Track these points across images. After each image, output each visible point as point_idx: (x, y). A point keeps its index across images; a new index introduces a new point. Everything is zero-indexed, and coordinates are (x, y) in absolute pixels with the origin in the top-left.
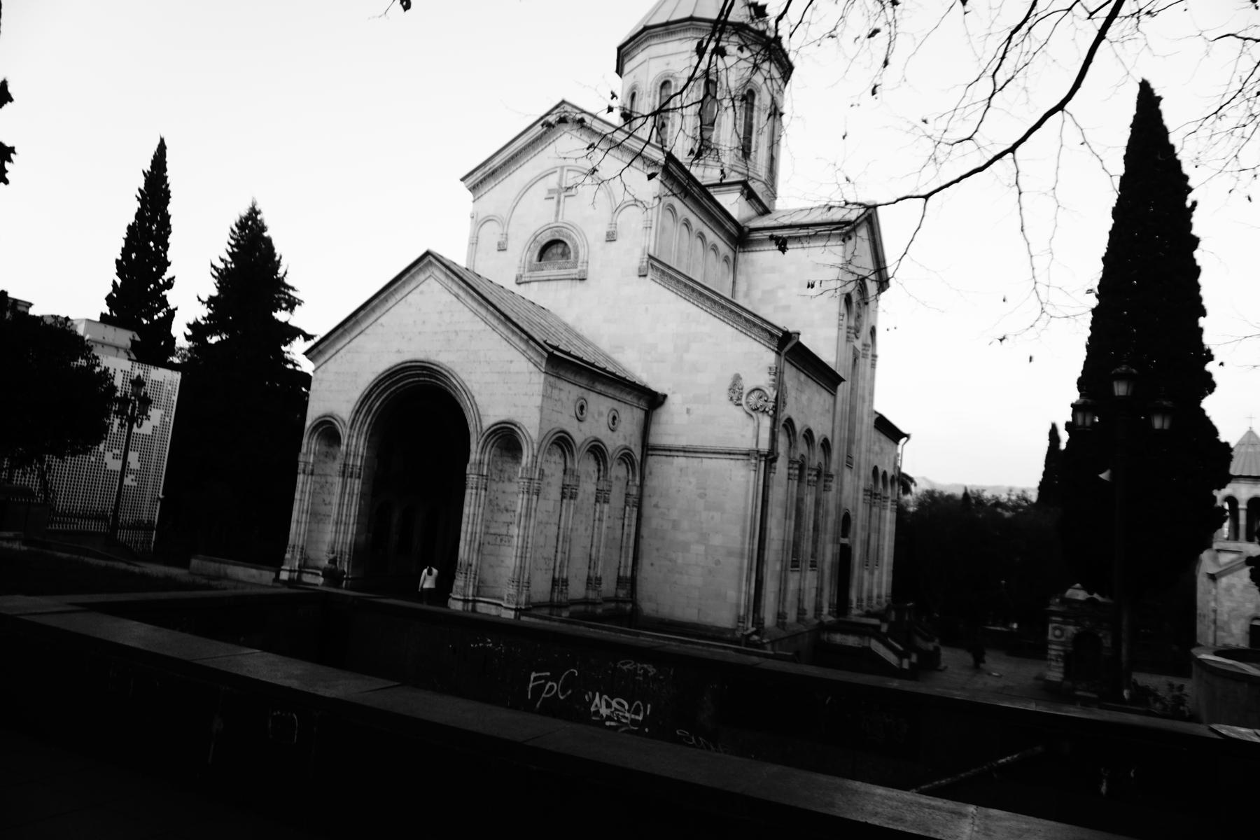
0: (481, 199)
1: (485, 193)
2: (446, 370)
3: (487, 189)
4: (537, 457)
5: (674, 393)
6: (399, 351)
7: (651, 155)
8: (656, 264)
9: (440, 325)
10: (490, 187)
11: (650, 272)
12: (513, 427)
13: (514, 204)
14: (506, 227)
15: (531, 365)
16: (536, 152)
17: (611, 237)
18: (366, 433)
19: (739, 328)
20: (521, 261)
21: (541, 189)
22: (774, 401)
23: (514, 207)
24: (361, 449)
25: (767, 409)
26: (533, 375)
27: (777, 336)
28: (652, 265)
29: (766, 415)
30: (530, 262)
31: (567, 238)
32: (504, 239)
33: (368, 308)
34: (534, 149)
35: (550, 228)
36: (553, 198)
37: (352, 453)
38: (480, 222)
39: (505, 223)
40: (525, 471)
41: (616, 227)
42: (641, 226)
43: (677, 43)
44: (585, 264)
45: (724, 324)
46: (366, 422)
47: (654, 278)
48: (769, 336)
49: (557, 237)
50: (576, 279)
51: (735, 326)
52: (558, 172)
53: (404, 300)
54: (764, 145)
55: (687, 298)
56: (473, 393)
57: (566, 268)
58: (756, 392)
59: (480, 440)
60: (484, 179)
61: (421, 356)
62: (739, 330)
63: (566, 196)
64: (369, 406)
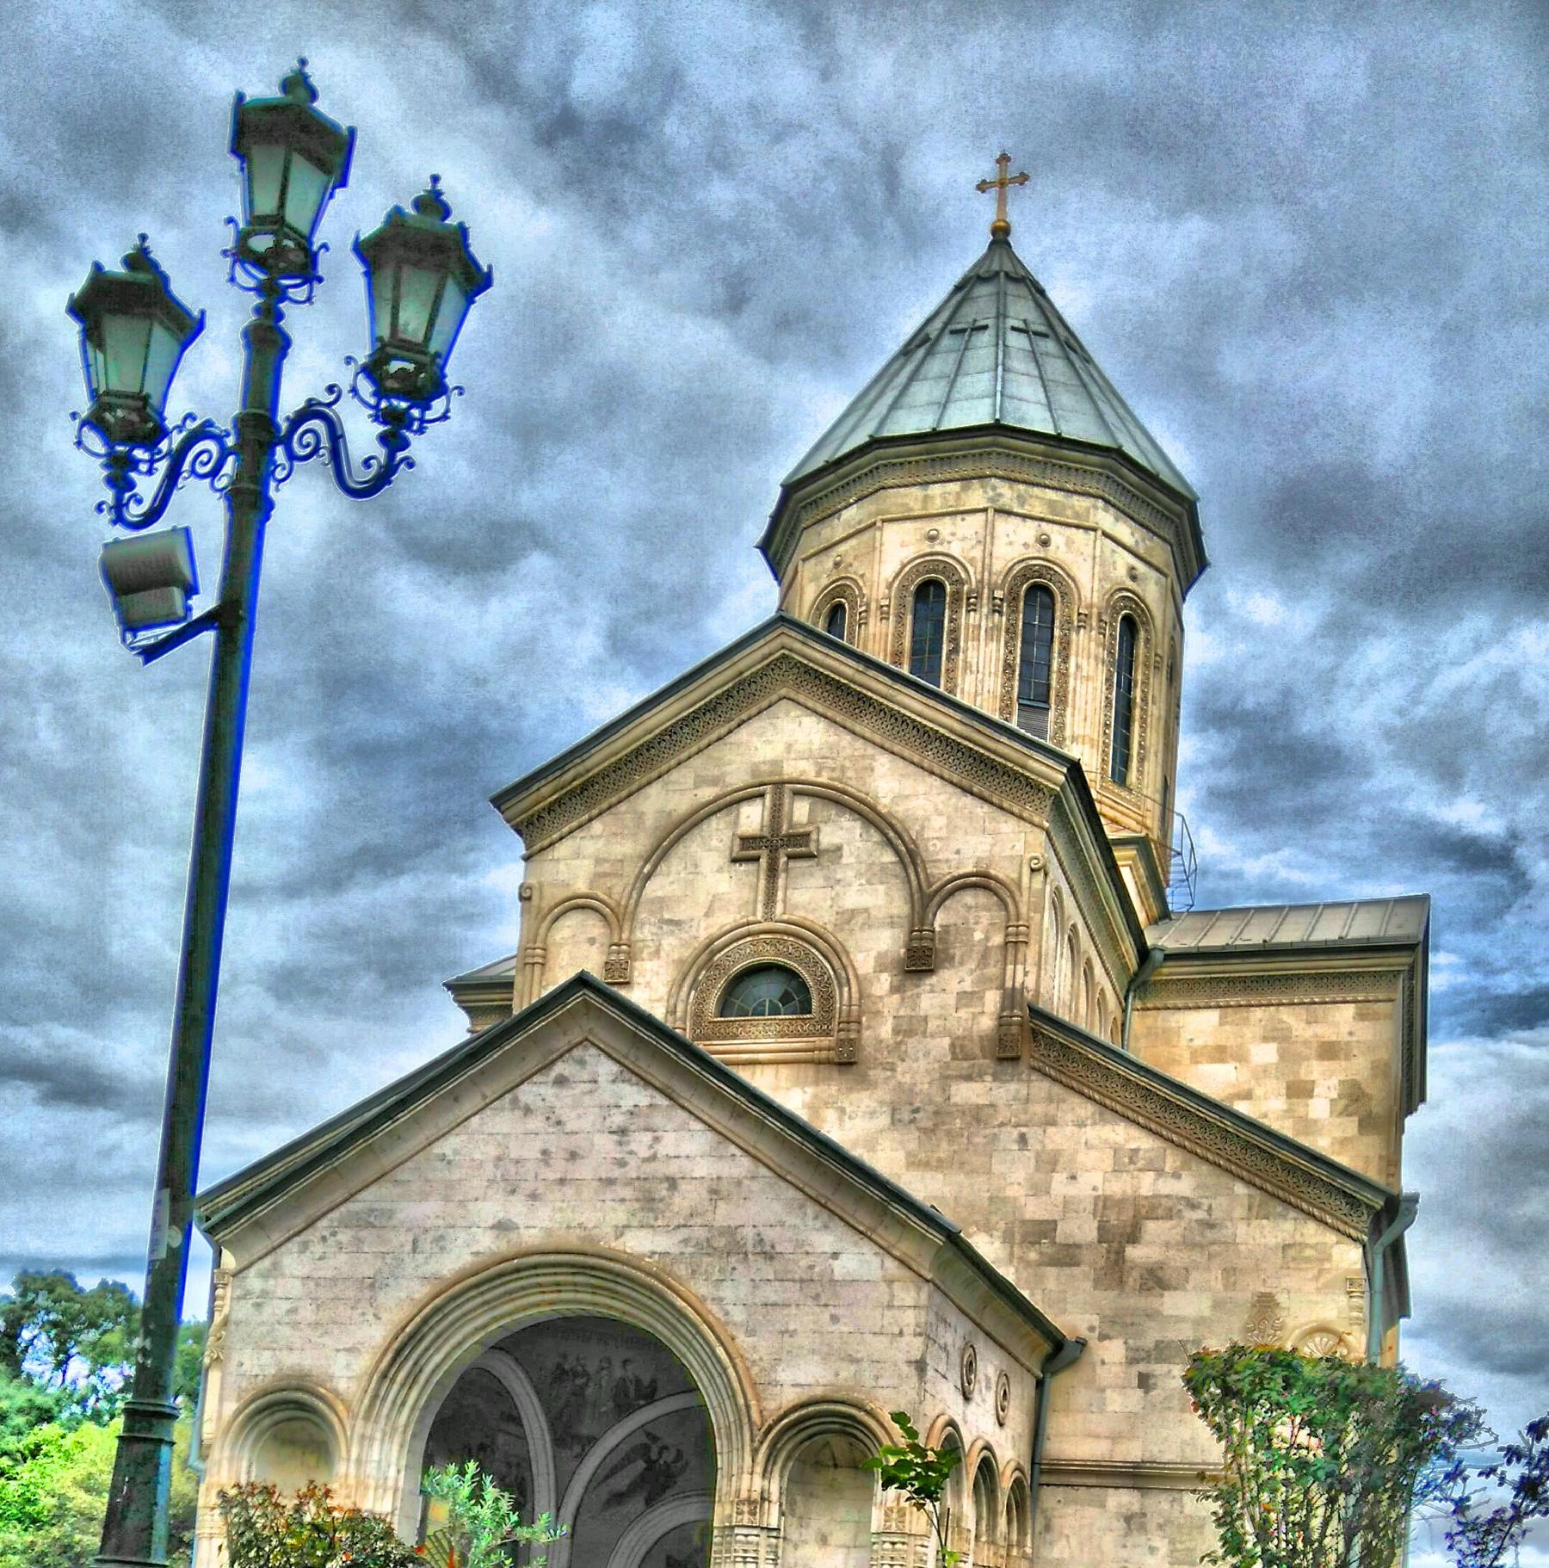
0: (549, 855)
1: (561, 839)
2: (648, 1274)
3: (566, 830)
6: (502, 1227)
8: (1048, 1030)
9: (622, 1163)
10: (575, 824)
11: (1025, 1050)
12: (853, 1411)
14: (626, 926)
15: (891, 1264)
18: (405, 1432)
19: (1269, 1187)
20: (674, 1012)
23: (649, 877)
24: (392, 1472)
26: (896, 1285)
27: (1368, 1206)
28: (1035, 1033)
30: (698, 1016)
32: (622, 957)
36: (756, 859)
37: (372, 1483)
38: (551, 910)
40: (894, 1516)
41: (932, 940)
42: (997, 939)
43: (954, 487)
44: (854, 1026)
45: (1225, 1179)
46: (403, 1404)
47: (1036, 1064)
48: (1346, 1209)
49: (769, 957)
50: (828, 1062)
51: (1258, 1181)
52: (768, 797)
55: (1130, 1114)
56: (731, 1330)
57: (800, 1036)
59: (762, 1443)
60: (559, 802)
61: (573, 1240)
62: (1266, 1191)
63: (791, 857)
64: (415, 1364)
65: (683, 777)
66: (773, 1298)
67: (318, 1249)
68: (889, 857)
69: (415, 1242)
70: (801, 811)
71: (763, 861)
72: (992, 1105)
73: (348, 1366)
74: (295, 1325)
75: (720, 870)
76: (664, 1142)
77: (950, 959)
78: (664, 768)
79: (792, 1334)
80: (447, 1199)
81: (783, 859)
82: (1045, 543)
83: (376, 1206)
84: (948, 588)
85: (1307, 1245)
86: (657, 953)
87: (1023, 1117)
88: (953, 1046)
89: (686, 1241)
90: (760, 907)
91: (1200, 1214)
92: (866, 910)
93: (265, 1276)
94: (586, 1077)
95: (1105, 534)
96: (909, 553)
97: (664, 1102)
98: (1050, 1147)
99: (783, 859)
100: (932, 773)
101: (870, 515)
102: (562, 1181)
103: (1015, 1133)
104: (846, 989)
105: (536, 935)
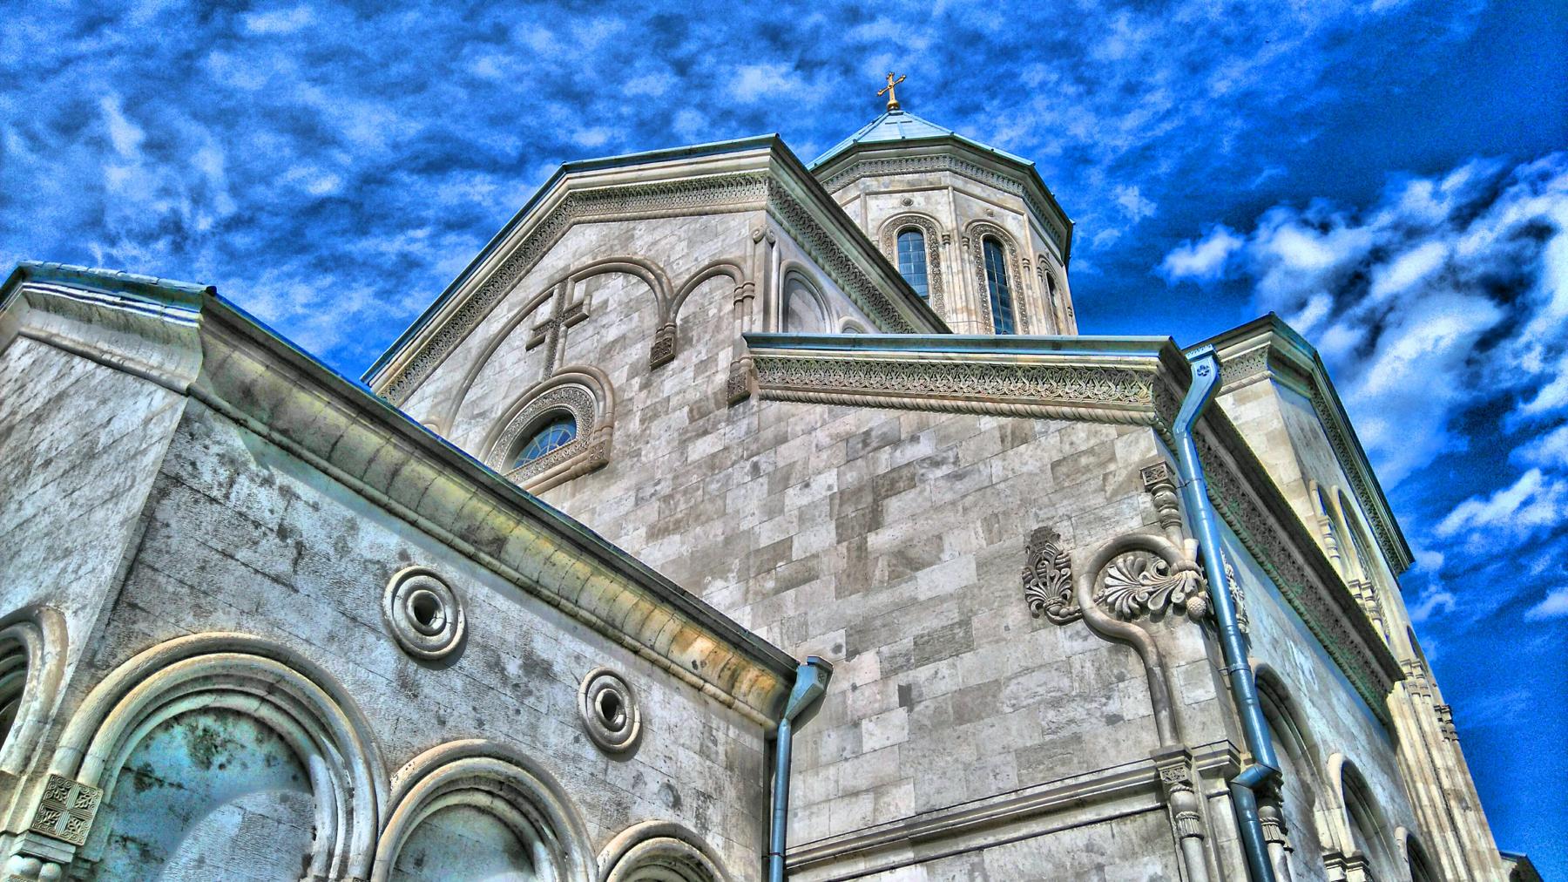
4: (60, 722)
5: (852, 654)
7: (738, 168)
17: (662, 356)
21: (523, 334)
22: (1196, 565)
25: (1177, 597)
29: (1179, 619)
31: (568, 399)
34: (512, 276)
35: (533, 397)
36: (542, 341)
42: (729, 306)
49: (546, 405)
50: (584, 472)
54: (1039, 321)
58: (1120, 561)
60: (413, 365)
63: (569, 326)
72: (726, 449)
77: (689, 341)
81: (563, 328)
82: (908, 203)
85: (1084, 453)
87: (754, 447)
88: (691, 411)
91: (945, 470)
95: (954, 189)
98: (781, 464)
99: (563, 328)
103: (748, 465)
104: (601, 404)
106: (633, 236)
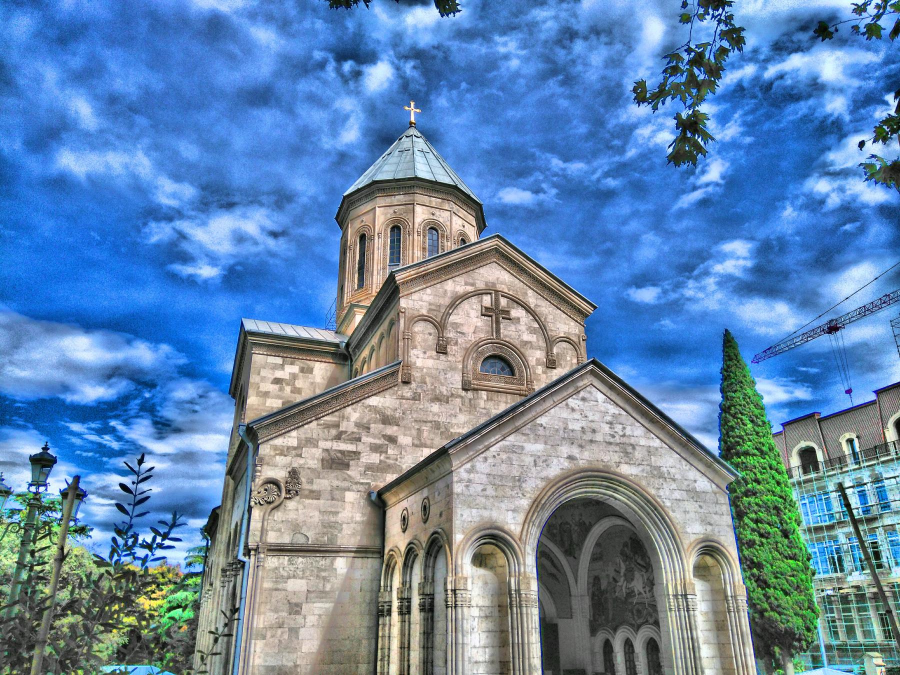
3: (417, 289)
7: (579, 305)
10: (421, 288)
13: (450, 311)
15: (714, 486)
16: (468, 269)
30: (475, 370)
33: (528, 406)
34: (465, 267)
36: (491, 316)
39: (440, 326)
49: (498, 352)
53: (564, 403)
60: (415, 278)
61: (601, 466)
63: (503, 318)
65: (461, 280)
66: (679, 497)
67: (490, 460)
68: (536, 325)
69: (535, 461)
70: (503, 302)
71: (494, 317)
73: (514, 518)
74: (487, 497)
75: (477, 317)
76: (627, 429)
78: (454, 275)
79: (688, 512)
80: (546, 443)
82: (464, 226)
83: (515, 443)
84: (440, 232)
86: (456, 343)
89: (643, 470)
90: (494, 334)
92: (530, 342)
93: (469, 471)
94: (593, 399)
96: (426, 217)
97: (625, 413)
100: (547, 300)
101: (411, 200)
102: (591, 441)
105: (408, 328)
106: (527, 294)
